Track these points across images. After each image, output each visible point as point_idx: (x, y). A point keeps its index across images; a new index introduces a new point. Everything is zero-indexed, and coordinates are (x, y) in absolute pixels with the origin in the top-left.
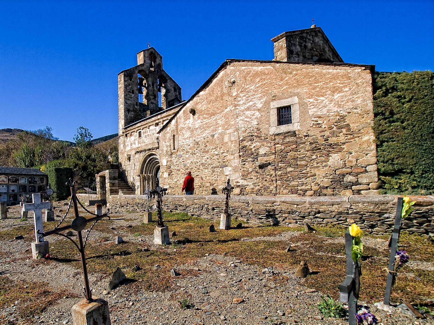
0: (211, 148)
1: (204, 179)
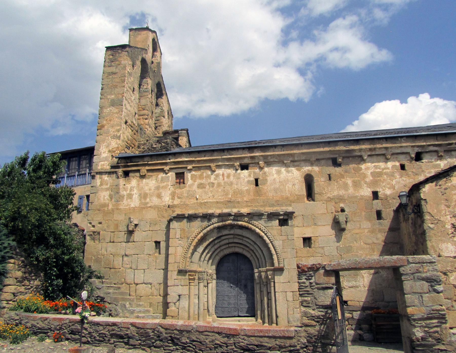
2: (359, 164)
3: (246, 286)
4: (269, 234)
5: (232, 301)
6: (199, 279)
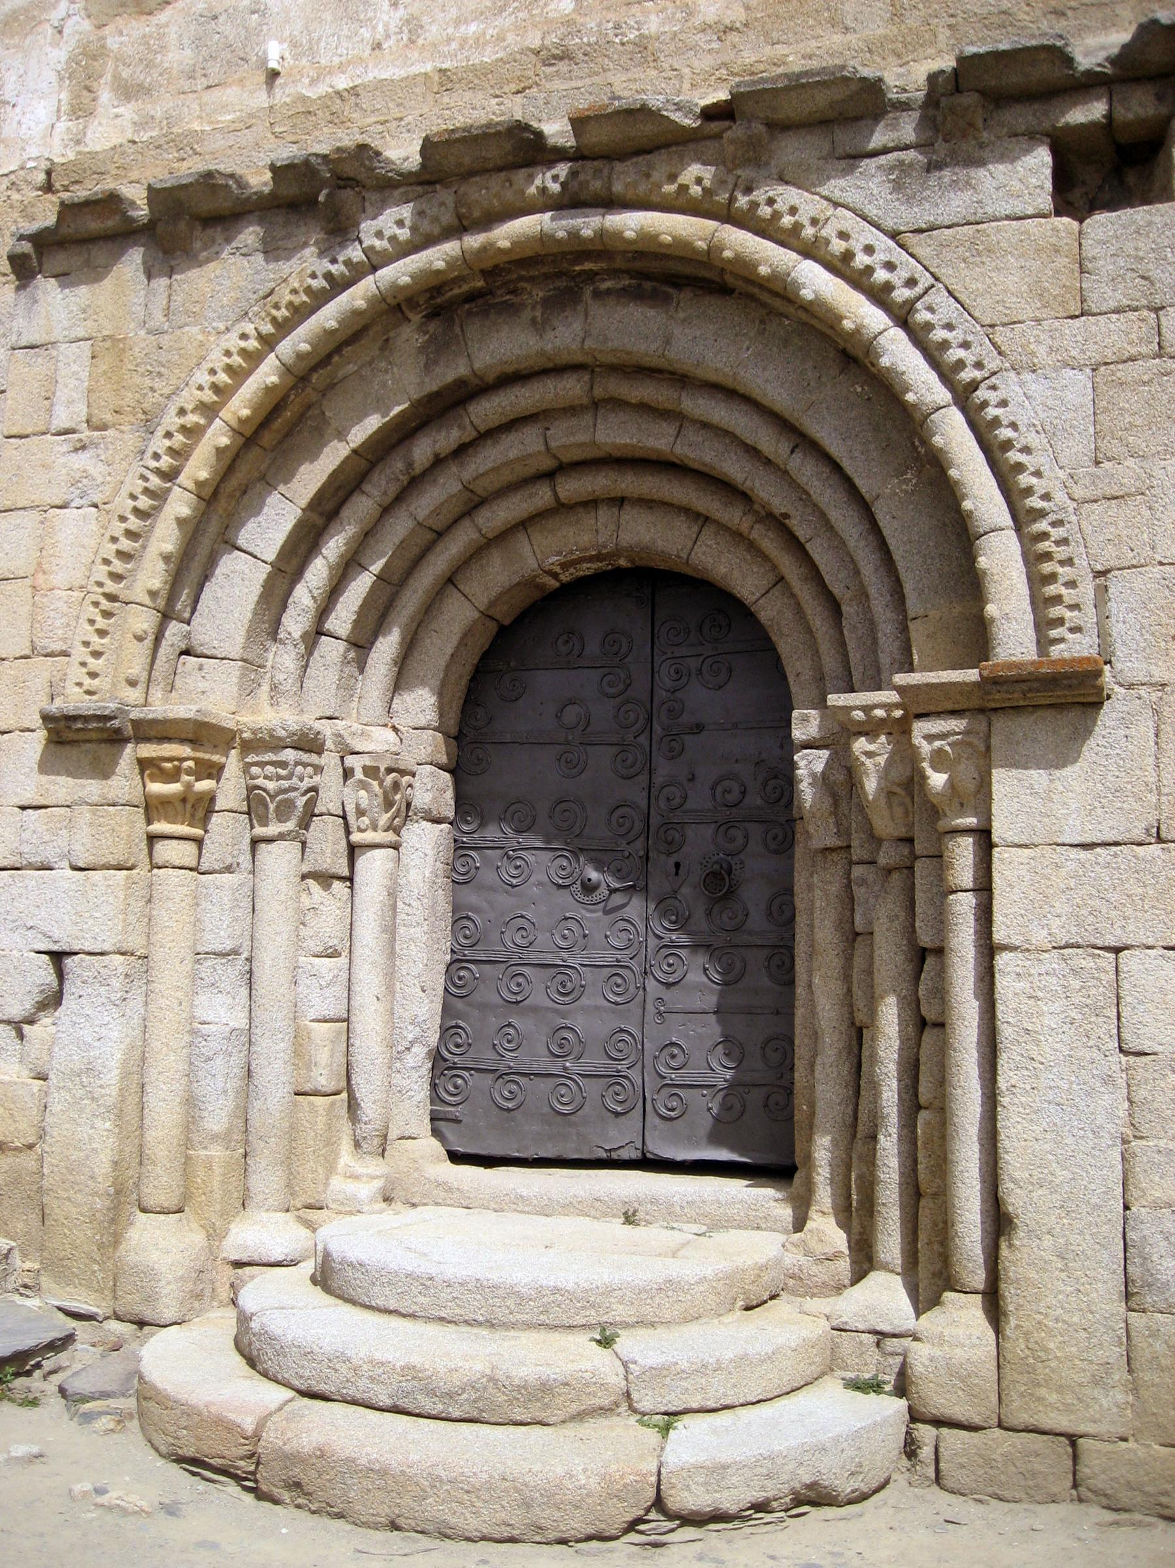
3: (720, 884)
4: (938, 311)
5: (591, 1019)
6: (255, 806)
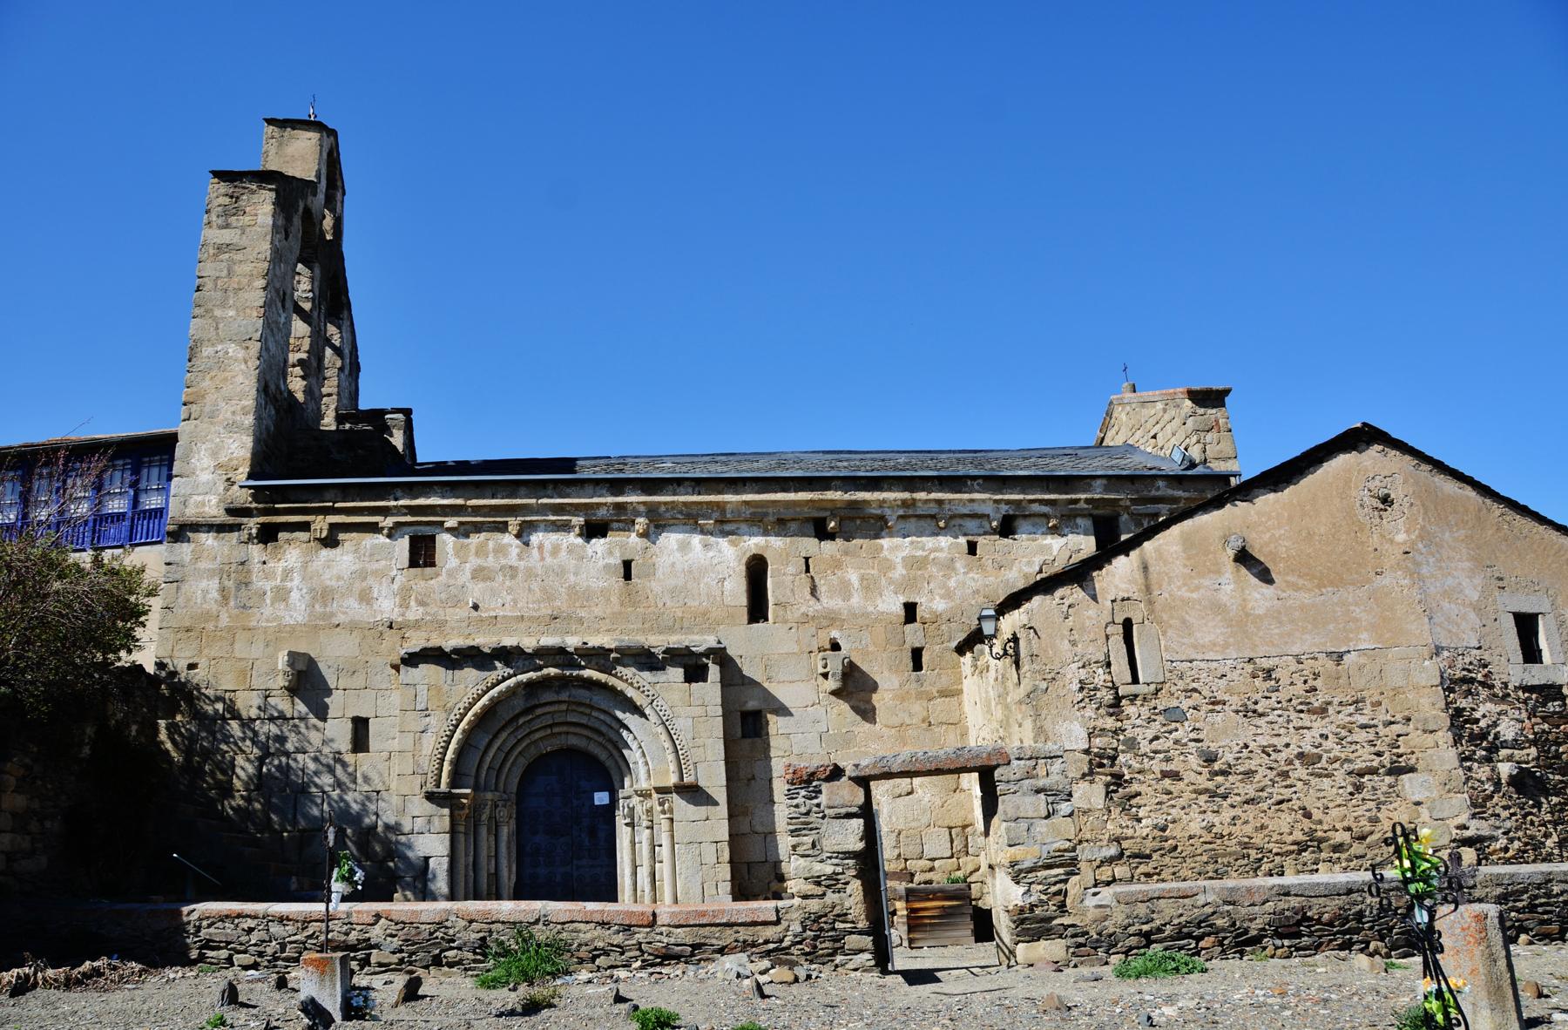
0: (1336, 700)
1: (1317, 814)
2: (877, 536)
